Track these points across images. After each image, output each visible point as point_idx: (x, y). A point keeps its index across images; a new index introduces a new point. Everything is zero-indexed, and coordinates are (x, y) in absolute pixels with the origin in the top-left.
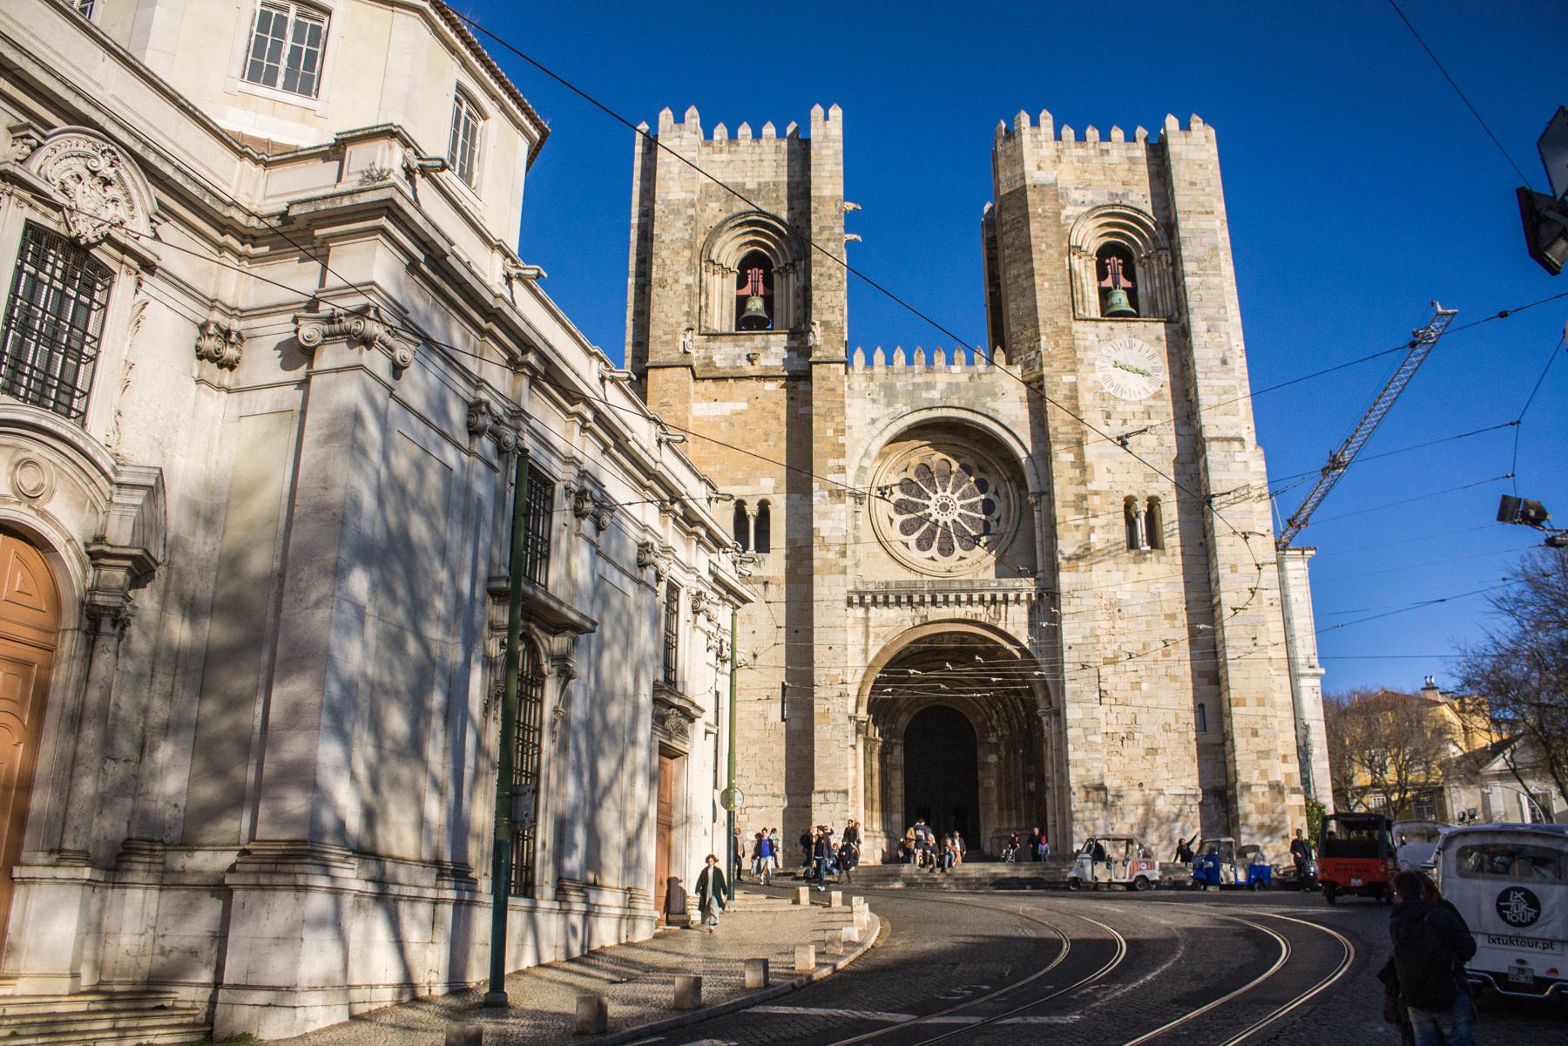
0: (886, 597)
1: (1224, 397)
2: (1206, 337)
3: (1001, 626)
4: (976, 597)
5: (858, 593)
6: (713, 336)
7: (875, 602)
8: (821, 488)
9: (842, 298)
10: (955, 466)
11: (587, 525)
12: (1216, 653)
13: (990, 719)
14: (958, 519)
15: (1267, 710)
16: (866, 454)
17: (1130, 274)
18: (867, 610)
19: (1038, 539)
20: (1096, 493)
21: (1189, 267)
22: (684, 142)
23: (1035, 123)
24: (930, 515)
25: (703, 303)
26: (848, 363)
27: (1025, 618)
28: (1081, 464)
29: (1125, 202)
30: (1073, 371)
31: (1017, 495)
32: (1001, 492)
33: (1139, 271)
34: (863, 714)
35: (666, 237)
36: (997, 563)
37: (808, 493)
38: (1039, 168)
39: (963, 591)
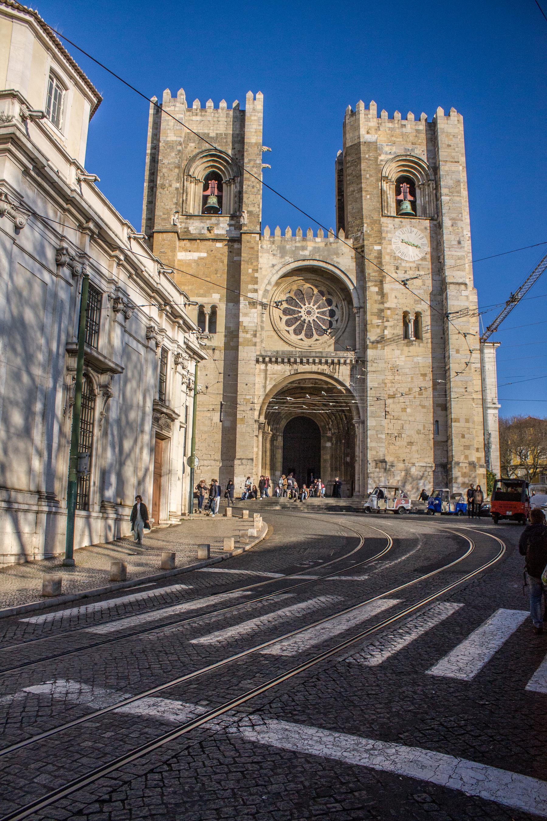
0: (277, 359)
1: (459, 261)
2: (451, 229)
3: (336, 376)
4: (323, 360)
5: (262, 356)
6: (190, 216)
7: (270, 361)
8: (244, 300)
9: (259, 199)
10: (316, 291)
11: (120, 316)
12: (446, 395)
13: (328, 424)
14: (316, 320)
15: (470, 425)
16: (269, 283)
17: (413, 193)
18: (266, 366)
19: (357, 332)
20: (389, 309)
21: (444, 191)
22: (177, 109)
23: (367, 107)
24: (301, 316)
25: (184, 198)
26: (261, 234)
27: (348, 372)
28: (382, 293)
29: (412, 154)
30: (380, 244)
31: (347, 309)
32: (339, 306)
33: (418, 191)
34: (262, 419)
35: (166, 161)
36: (336, 342)
37: (238, 302)
38: (368, 133)
39: (317, 357)
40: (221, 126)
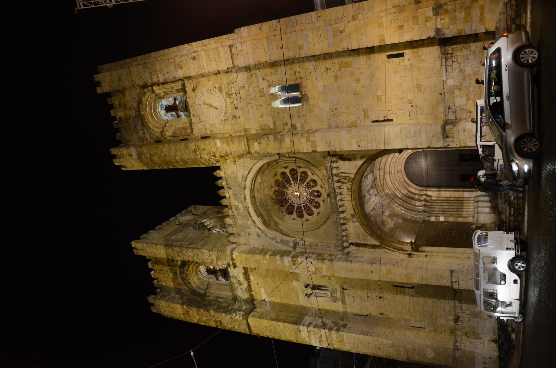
1: (210, 56)
2: (184, 69)
3: (352, 176)
6: (235, 298)
20: (275, 123)
27: (347, 162)
32: (285, 165)
38: (131, 155)
39: (335, 198)
40: (164, 269)
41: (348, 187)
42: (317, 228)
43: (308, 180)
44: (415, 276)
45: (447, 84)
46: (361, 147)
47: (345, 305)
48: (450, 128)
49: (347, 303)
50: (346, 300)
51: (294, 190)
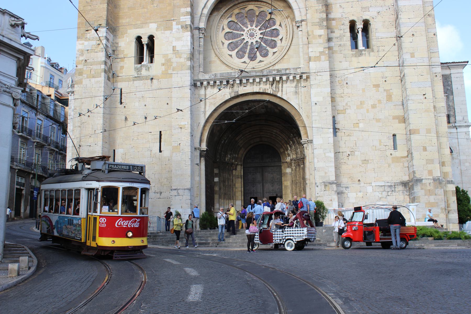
0: (215, 82)
3: (279, 95)
4: (264, 79)
8: (177, 24)
12: (403, 105)
20: (333, 19)
24: (244, 39)
27: (293, 89)
32: (283, 25)
41: (268, 89)
42: (216, 54)
43: (268, 48)
44: (181, 153)
45: (369, 187)
46: (315, 105)
47: (132, 80)
48: (333, 188)
49: (135, 82)
50: (138, 81)
51: (256, 32)
